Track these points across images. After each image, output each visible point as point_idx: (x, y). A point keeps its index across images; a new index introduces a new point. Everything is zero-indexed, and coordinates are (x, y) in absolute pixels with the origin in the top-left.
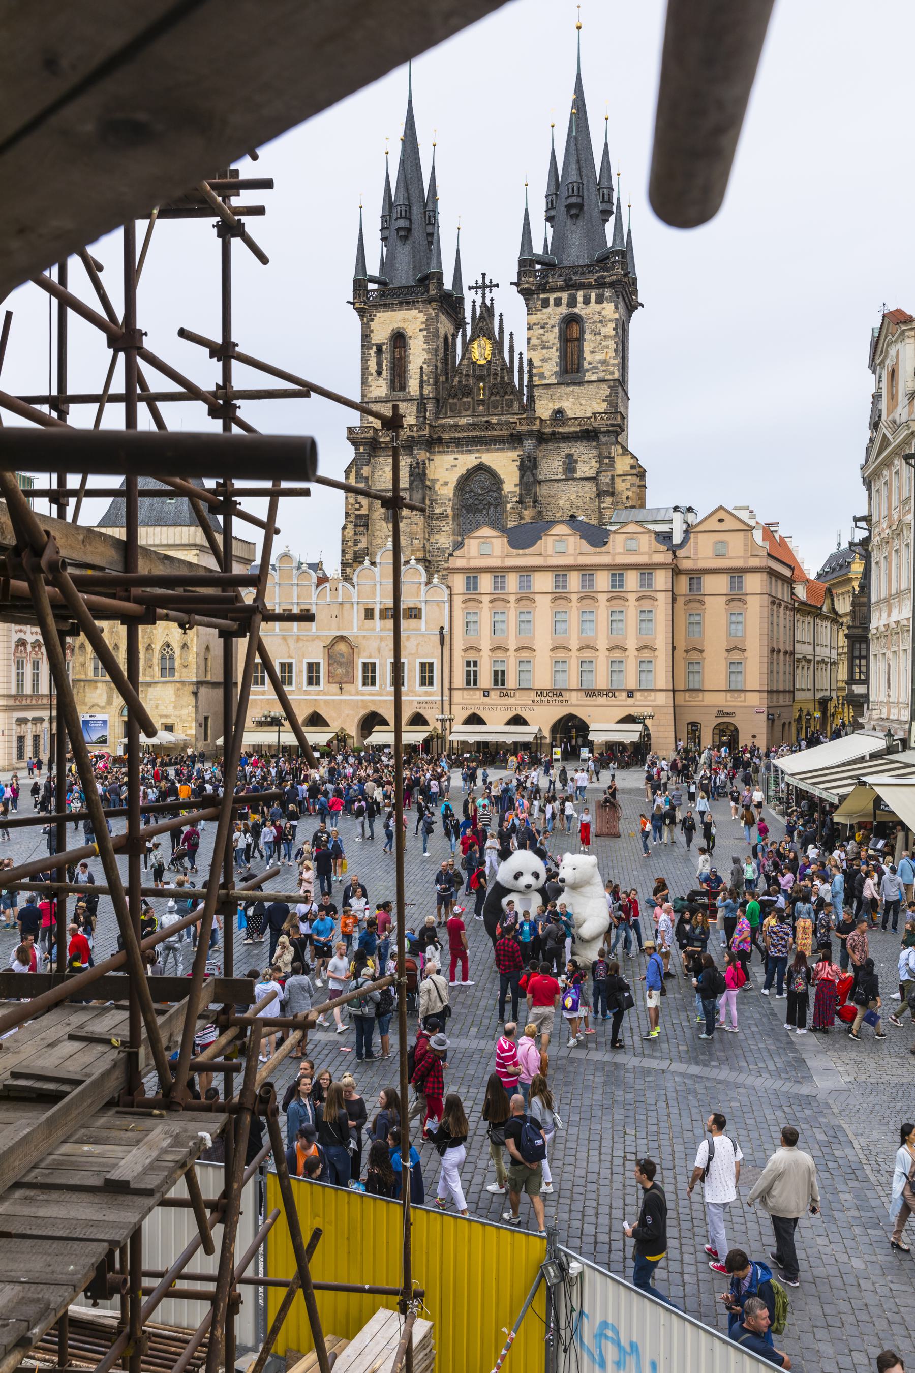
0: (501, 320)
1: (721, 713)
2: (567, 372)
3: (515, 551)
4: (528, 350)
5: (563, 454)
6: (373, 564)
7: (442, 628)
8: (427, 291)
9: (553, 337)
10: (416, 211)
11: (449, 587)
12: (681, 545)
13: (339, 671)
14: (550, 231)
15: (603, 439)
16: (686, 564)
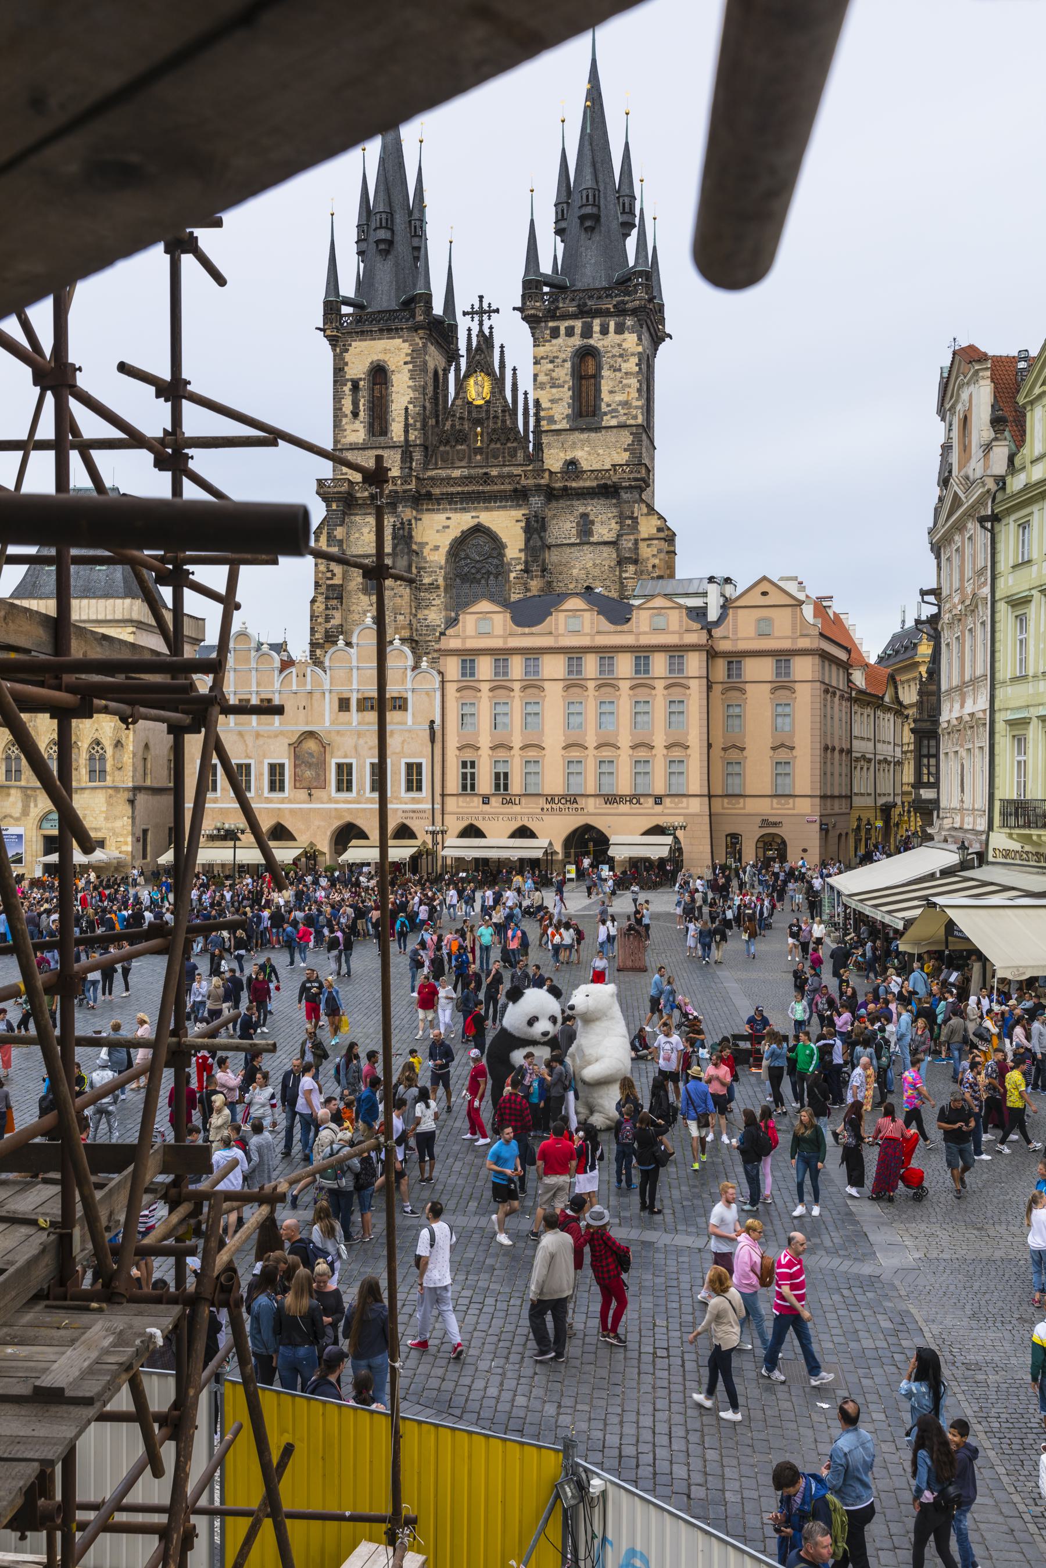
0: (502, 353)
1: (765, 823)
2: (581, 415)
3: (520, 630)
4: (535, 389)
5: (577, 513)
6: (348, 644)
7: (432, 722)
8: (413, 316)
9: (563, 374)
10: (400, 219)
11: (440, 673)
12: (718, 623)
13: (308, 773)
14: (561, 247)
15: (625, 496)
16: (724, 646)
